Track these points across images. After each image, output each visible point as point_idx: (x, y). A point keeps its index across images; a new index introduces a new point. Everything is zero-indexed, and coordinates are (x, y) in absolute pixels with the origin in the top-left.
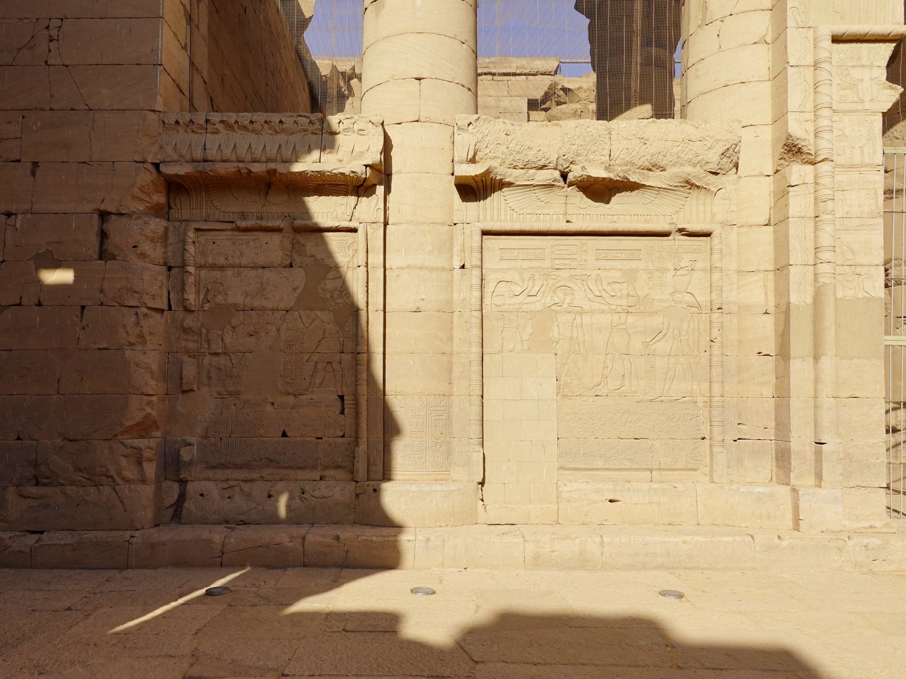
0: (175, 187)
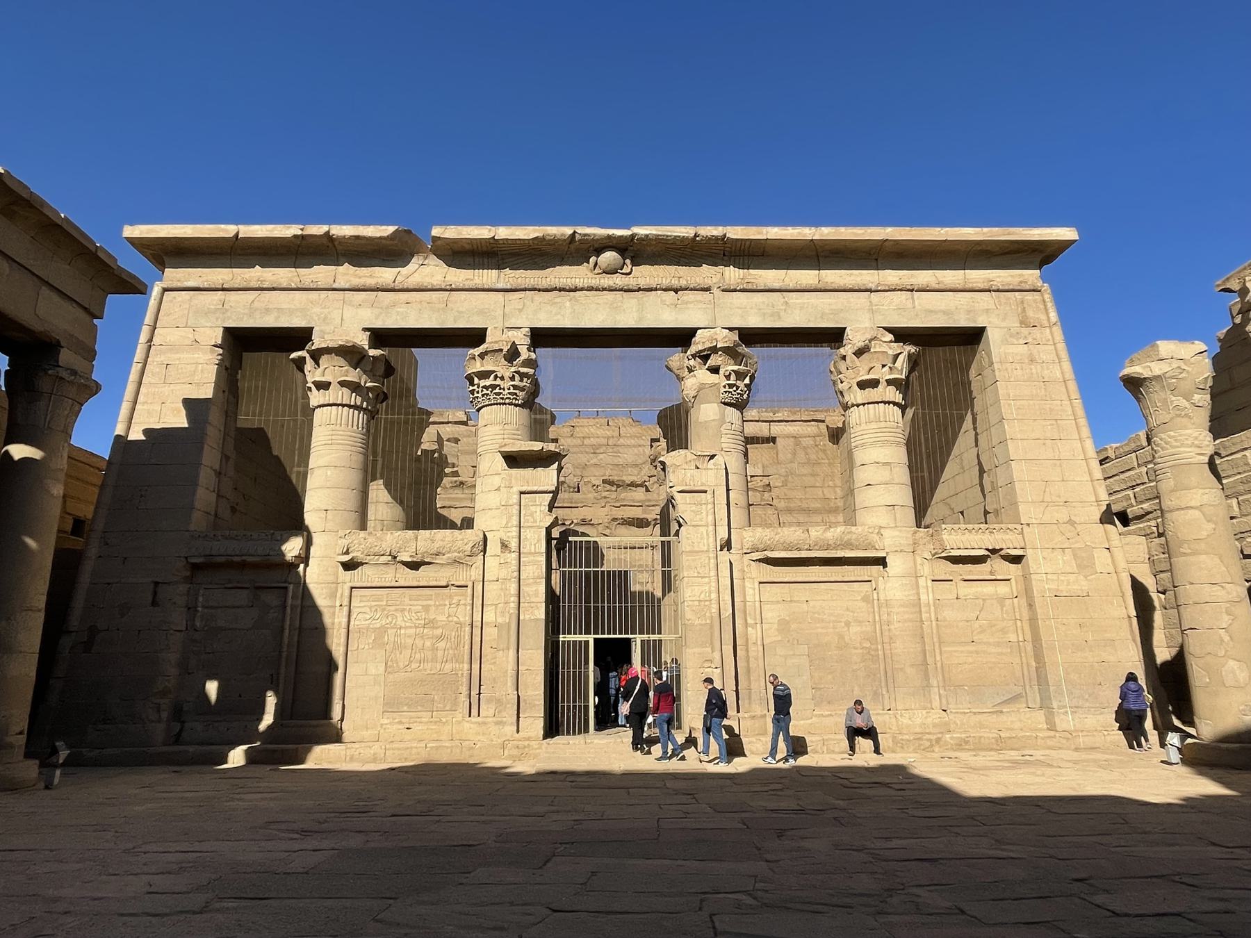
0: (195, 567)
